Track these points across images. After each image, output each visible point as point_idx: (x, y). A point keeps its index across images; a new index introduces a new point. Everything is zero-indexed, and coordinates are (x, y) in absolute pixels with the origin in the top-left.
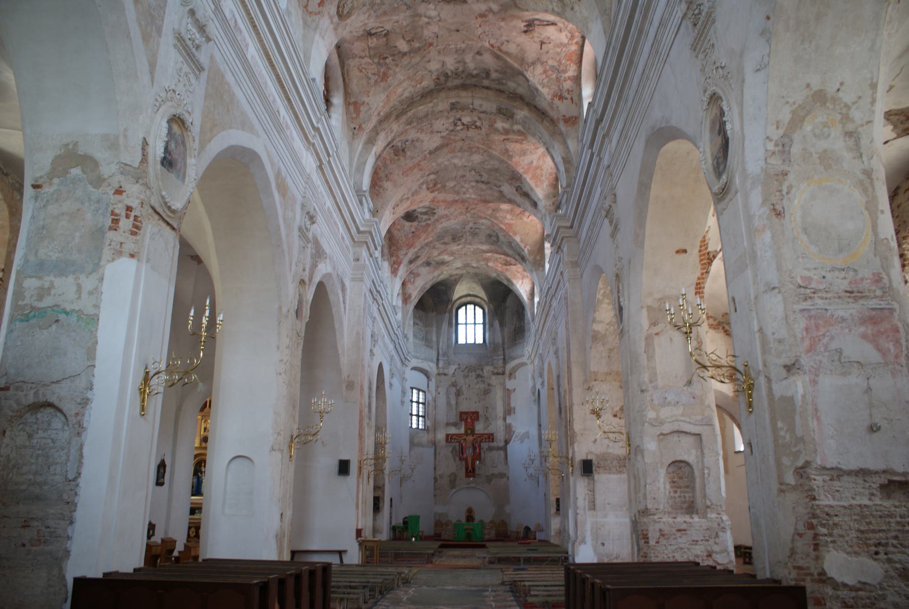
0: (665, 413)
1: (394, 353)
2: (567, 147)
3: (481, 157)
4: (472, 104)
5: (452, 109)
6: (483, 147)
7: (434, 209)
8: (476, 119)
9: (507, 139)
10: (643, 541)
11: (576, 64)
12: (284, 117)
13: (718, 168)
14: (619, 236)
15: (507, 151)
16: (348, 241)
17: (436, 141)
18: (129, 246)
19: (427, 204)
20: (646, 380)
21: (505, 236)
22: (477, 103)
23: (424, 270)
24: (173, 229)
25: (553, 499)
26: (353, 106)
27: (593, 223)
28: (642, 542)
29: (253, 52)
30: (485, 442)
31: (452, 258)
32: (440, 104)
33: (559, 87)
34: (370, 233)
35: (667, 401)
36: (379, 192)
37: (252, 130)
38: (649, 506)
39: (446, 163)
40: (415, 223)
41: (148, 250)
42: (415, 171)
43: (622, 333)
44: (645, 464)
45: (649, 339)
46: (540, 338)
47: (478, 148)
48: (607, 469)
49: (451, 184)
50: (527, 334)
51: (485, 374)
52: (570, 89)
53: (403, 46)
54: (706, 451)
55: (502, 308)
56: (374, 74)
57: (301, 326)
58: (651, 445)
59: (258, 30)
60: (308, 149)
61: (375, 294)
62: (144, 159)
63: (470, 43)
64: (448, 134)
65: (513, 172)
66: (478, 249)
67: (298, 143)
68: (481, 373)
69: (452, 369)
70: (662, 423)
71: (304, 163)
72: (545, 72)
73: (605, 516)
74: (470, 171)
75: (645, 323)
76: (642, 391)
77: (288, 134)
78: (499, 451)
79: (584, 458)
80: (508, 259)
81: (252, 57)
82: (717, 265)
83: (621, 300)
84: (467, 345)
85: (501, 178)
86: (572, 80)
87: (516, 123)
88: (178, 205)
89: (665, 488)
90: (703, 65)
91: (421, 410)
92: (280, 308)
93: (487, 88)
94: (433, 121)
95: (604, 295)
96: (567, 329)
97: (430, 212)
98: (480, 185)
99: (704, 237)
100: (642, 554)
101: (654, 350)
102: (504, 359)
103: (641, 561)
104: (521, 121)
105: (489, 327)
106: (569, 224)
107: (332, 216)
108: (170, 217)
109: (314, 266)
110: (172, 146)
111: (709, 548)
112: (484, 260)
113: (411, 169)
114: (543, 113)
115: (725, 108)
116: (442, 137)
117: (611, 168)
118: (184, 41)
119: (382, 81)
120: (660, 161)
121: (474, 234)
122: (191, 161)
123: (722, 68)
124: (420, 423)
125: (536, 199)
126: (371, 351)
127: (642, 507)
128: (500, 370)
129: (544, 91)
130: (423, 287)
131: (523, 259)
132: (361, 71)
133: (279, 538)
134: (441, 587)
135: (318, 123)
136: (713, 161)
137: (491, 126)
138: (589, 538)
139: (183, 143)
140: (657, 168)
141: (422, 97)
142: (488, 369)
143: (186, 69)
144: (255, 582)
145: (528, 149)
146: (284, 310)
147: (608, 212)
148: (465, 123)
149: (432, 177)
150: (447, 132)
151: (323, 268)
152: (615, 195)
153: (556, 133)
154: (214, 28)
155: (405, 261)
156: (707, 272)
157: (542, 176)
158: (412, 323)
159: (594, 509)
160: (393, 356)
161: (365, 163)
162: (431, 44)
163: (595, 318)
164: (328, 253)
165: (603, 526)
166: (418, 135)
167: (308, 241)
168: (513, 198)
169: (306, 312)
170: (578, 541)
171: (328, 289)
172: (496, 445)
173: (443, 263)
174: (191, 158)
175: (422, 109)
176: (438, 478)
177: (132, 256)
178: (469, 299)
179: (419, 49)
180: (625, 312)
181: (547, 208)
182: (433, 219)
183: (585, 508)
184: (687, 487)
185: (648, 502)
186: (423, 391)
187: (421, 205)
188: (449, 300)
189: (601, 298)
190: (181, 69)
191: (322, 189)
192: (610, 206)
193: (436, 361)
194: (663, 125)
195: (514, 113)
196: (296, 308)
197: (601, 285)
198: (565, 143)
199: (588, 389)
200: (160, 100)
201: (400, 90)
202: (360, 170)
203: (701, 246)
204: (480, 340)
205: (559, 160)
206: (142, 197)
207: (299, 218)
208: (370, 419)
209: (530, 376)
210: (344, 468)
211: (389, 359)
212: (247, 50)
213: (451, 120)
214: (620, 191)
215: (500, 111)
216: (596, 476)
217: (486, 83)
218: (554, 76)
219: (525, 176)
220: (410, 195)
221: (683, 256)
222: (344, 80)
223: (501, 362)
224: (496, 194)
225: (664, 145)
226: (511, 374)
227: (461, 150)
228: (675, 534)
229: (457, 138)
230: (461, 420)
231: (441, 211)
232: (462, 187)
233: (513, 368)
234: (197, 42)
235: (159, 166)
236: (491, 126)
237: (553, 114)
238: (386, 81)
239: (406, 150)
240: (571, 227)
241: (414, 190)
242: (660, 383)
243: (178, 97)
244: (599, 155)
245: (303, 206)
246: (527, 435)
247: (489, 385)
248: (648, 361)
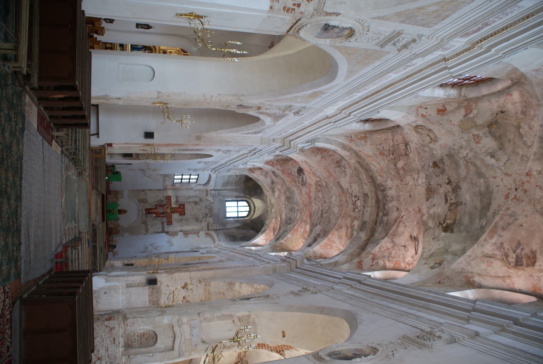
0: (186, 328)
1: (219, 164)
2: (344, 263)
3: (337, 213)
4: (368, 206)
5: (364, 194)
6: (343, 214)
7: (305, 186)
8: (359, 209)
9: (348, 228)
10: (107, 317)
11: (393, 267)
12: (356, 95)
13: (333, 354)
14: (292, 296)
15: (341, 228)
16: (284, 135)
17: (345, 185)
18: (277, 6)
19: (308, 181)
20: (206, 316)
21: (291, 228)
22: (369, 209)
23: (269, 180)
24: (288, 32)
25: (133, 262)
26: (364, 136)
27: (299, 281)
28: (107, 317)
29: (393, 76)
30: (167, 220)
31: (277, 197)
32: (367, 187)
33: (380, 257)
34: (290, 148)
35: (193, 329)
36: (314, 153)
37: (348, 77)
38: (129, 320)
39: (333, 192)
40: (296, 174)
41: (275, 17)
42: (327, 174)
43: (234, 300)
44: (155, 317)
45: (231, 316)
46: (230, 251)
47: (342, 211)
48: (151, 295)
49: (320, 195)
50: (232, 243)
52: (378, 264)
53: (400, 164)
54: (163, 354)
56: (383, 148)
57: (233, 108)
58: (166, 320)
59: (406, 79)
60: (338, 110)
61: (254, 152)
62: (328, 14)
63: (404, 204)
64: (350, 192)
65: (329, 232)
66: (282, 212)
67: (341, 104)
68: (208, 216)
69: (210, 198)
70: (180, 326)
71: (330, 107)
72: (388, 249)
73: (123, 294)
74: (328, 206)
75: (240, 314)
76: (199, 314)
77: (346, 98)
79: (158, 280)
80: (277, 231)
81: (390, 76)
82: (276, 356)
83: (254, 299)
84: (225, 207)
85: (324, 225)
86: (384, 265)
87: (357, 233)
88: (302, 34)
89: (140, 330)
90: (394, 343)
91: (185, 181)
92: (243, 95)
93: (377, 215)
94: (357, 184)
95: (256, 288)
96: (236, 267)
97: (304, 183)
98: (320, 213)
99: (293, 348)
100: (99, 317)
101: (224, 320)
102: (217, 230)
103: (94, 317)
104: (359, 235)
105: (236, 220)
106: (298, 266)
107: (299, 125)
108: (295, 29)
109: (269, 115)
110: (337, 30)
111: (103, 358)
112: (276, 216)
113: (329, 172)
114: (364, 249)
115: (369, 357)
116: (348, 189)
117: (332, 290)
118: (398, 36)
119: (379, 152)
120: (337, 319)
121: (291, 210)
122: (328, 41)
123: (393, 355)
124: (178, 181)
125: (312, 246)
126: (220, 150)
127: (128, 316)
128: (210, 228)
129: (377, 249)
130: (259, 180)
131: (277, 239)
132: (385, 140)
133: (105, 97)
134: (77, 195)
135: (354, 115)
136: (337, 351)
137: (355, 218)
138: (108, 284)
139: (338, 37)
140: (333, 318)
141: (371, 176)
142: (211, 220)
143: (382, 38)
144: (77, 83)
145: (342, 240)
146: (242, 98)
147: (306, 289)
148: (357, 202)
149: (324, 184)
150: (351, 192)
151: (268, 120)
152: (316, 293)
153: (352, 256)
154: (405, 53)
155: (274, 169)
156: (272, 351)
157: (327, 249)
158: (237, 174)
159: (127, 287)
160: (217, 163)
161: (331, 144)
162: (402, 181)
163: (243, 284)
164: (278, 123)
165: (117, 293)
166: (349, 175)
167: (284, 111)
168: (313, 232)
169: (241, 111)
170: (107, 278)
171: (256, 124)
173: (273, 192)
174: (330, 41)
175: (364, 176)
177: (271, 8)
178: (253, 208)
179: (399, 174)
180: (246, 301)
181: (308, 253)
182: (299, 185)
183: (128, 281)
184: (141, 343)
185: (132, 320)
187: (307, 178)
188: (251, 196)
189: (255, 287)
190: (381, 34)
191: (315, 119)
192: (309, 290)
194: (358, 321)
195: (363, 231)
196: (244, 105)
197: (262, 286)
198: (346, 262)
199: (200, 281)
200: (363, 22)
201: (374, 163)
202: (327, 141)
203: (287, 346)
204: (228, 215)
205: (337, 259)
206: (306, 13)
207: (297, 105)
208: (179, 150)
209: (207, 246)
210: (149, 135)
211: (215, 161)
212: (395, 73)
213: (358, 194)
214: (319, 296)
215: (364, 223)
216: (147, 287)
217: (381, 214)
218: (386, 254)
219: (326, 239)
220: (313, 171)
221: (281, 335)
222: (379, 130)
223: (216, 228)
224: (315, 222)
225: (347, 322)
226: (208, 234)
227: (341, 200)
228: (112, 337)
229: (347, 198)
230: (180, 205)
231: (304, 190)
232: (319, 202)
233: (212, 235)
234: (397, 44)
235: (324, 23)
236: (355, 218)
237: (363, 254)
238: (380, 155)
239: (340, 168)
240: (297, 268)
241: (316, 173)
242: (204, 324)
243: (365, 33)
244: (340, 282)
245: (304, 108)
246: (171, 245)
247: (201, 221)
248: (217, 317)
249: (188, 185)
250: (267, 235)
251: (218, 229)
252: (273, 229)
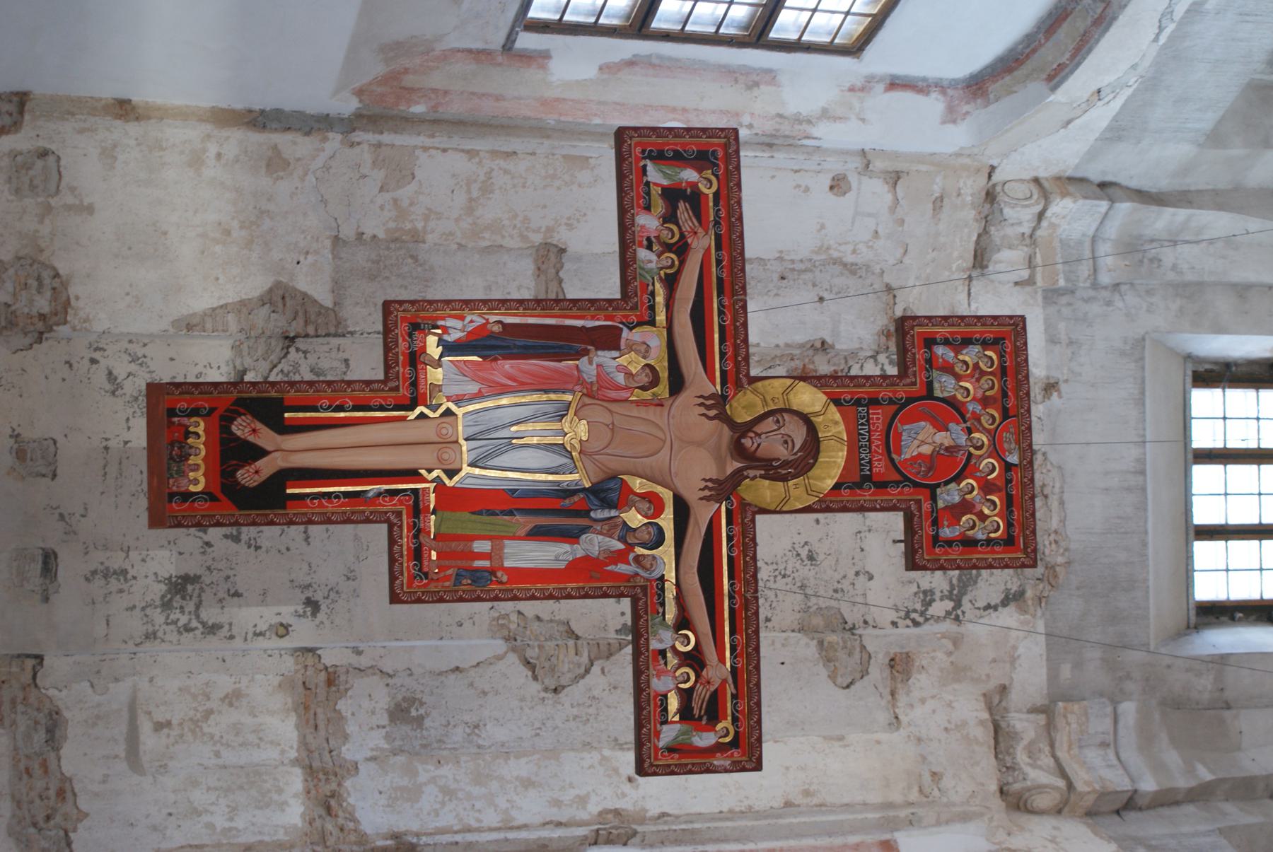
51: (979, 629)
78: (296, 781)
102: (1129, 804)
172: (349, 752)
176: (20, 141)
193: (1095, 173)
223: (1119, 781)
247: (900, 666)
249: (731, 73)
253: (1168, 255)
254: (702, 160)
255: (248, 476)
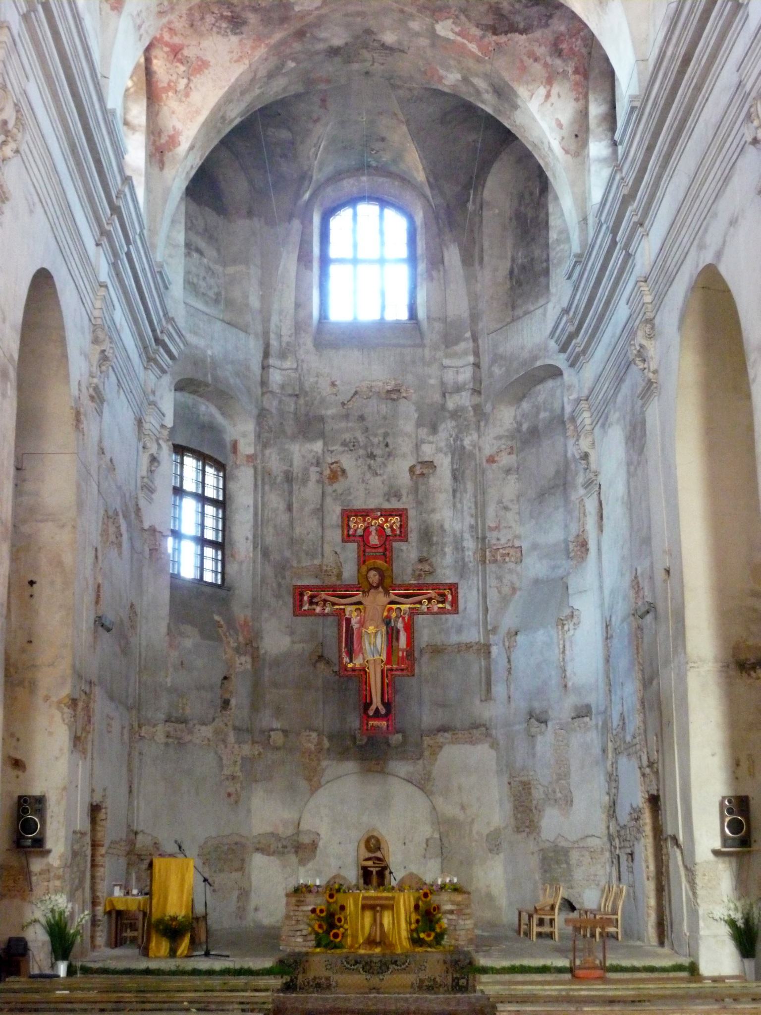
30: (429, 612)
55: (470, 206)
130: (217, 115)
186: (220, 466)
250: (524, 69)
251: (471, 359)
252: (495, 33)
253: (285, 339)
254: (301, 595)
255: (383, 711)
